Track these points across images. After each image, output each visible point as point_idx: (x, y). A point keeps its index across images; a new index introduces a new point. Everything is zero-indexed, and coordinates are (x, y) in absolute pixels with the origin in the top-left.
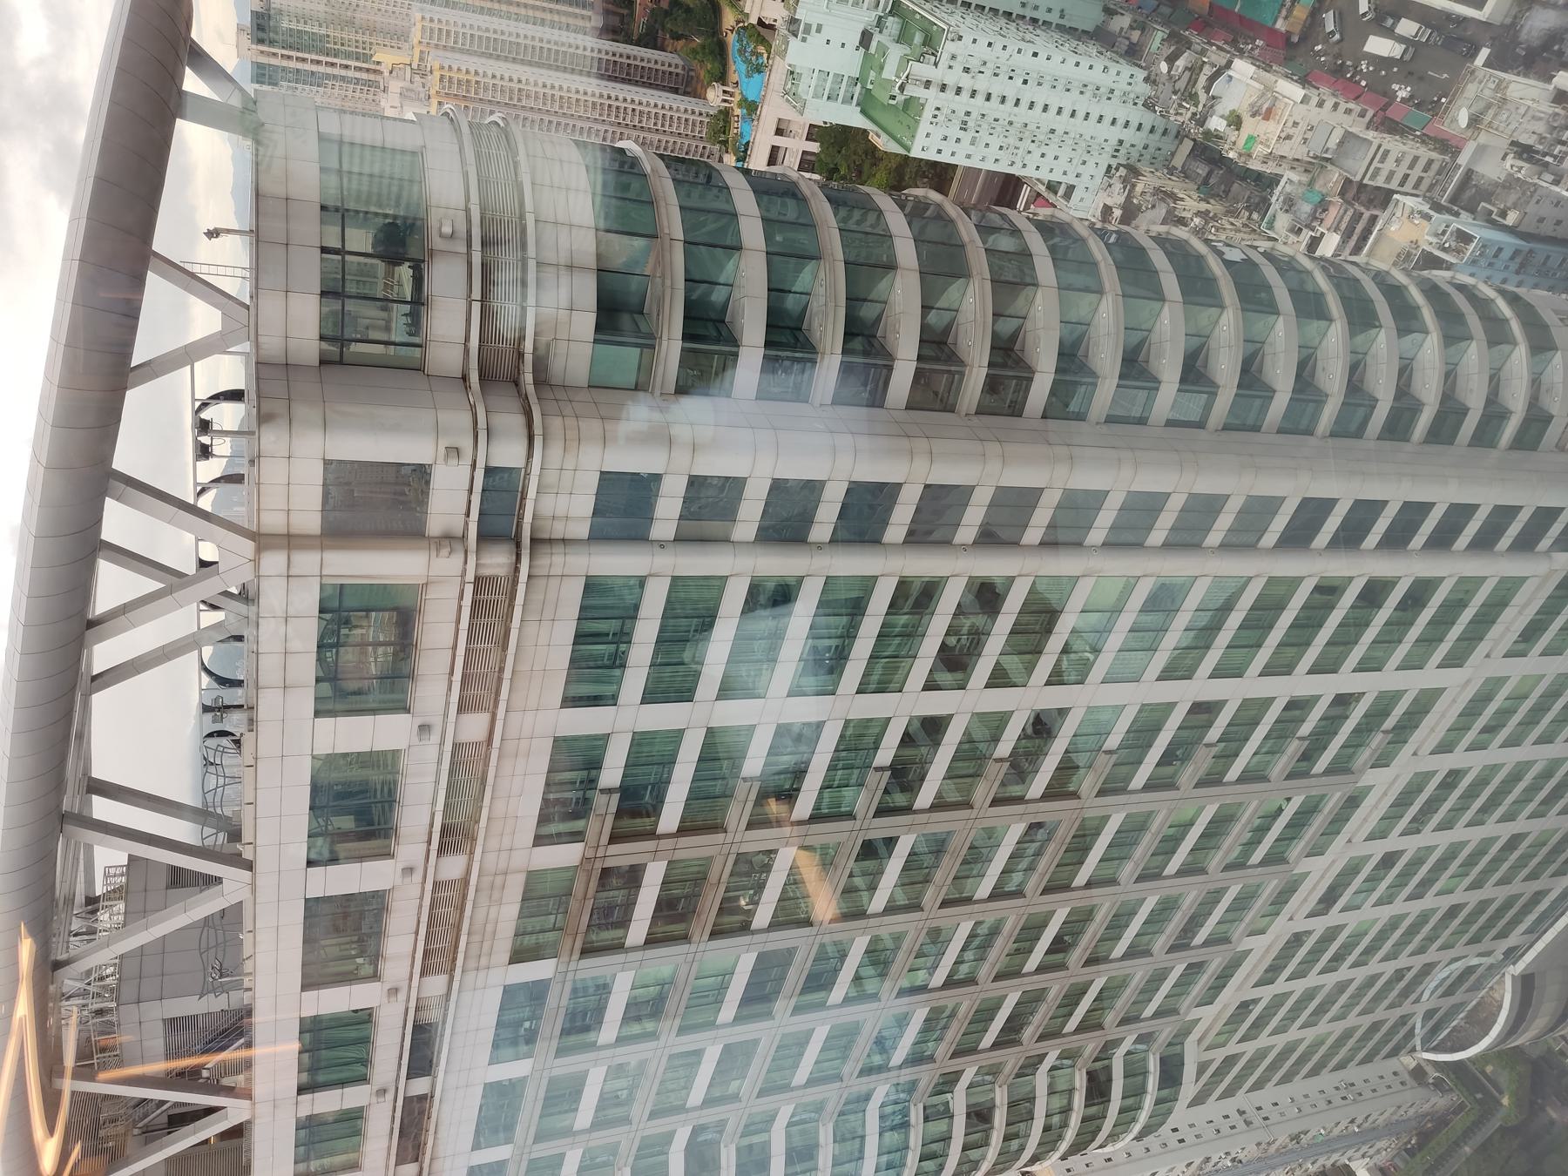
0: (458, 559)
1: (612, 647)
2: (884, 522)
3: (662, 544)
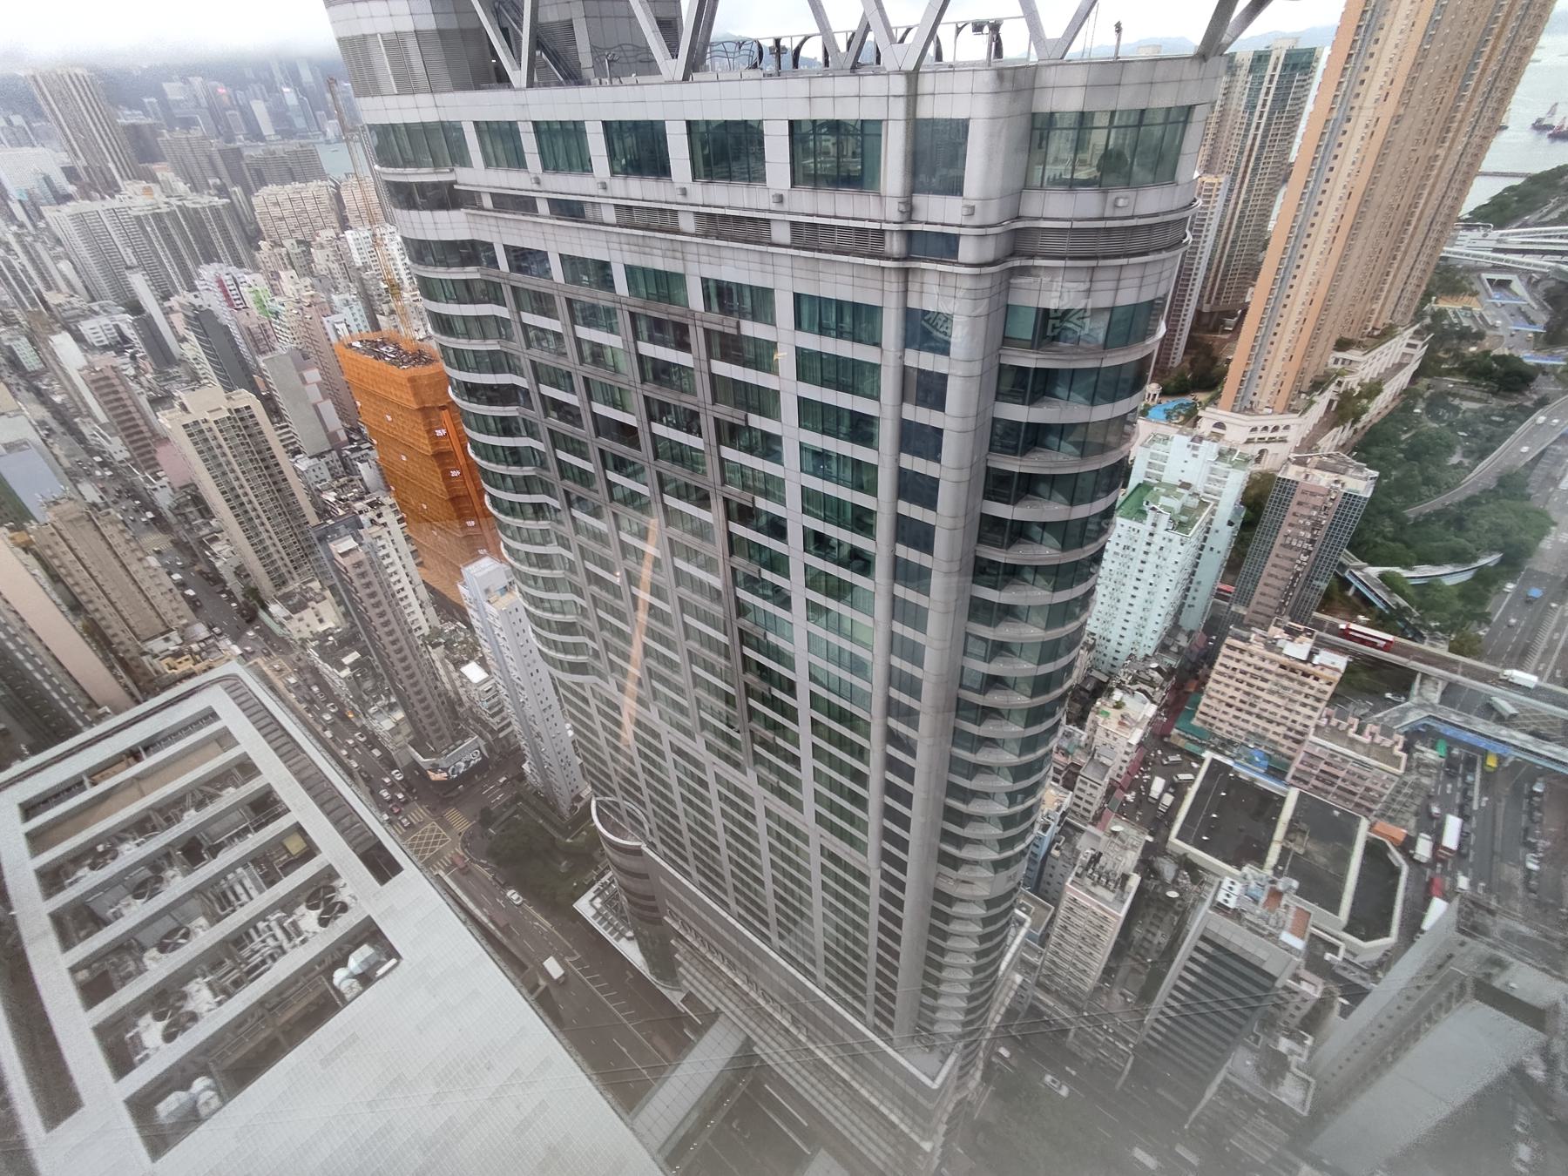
0: (896, 216)
1: (833, 325)
2: (911, 501)
3: (902, 357)
